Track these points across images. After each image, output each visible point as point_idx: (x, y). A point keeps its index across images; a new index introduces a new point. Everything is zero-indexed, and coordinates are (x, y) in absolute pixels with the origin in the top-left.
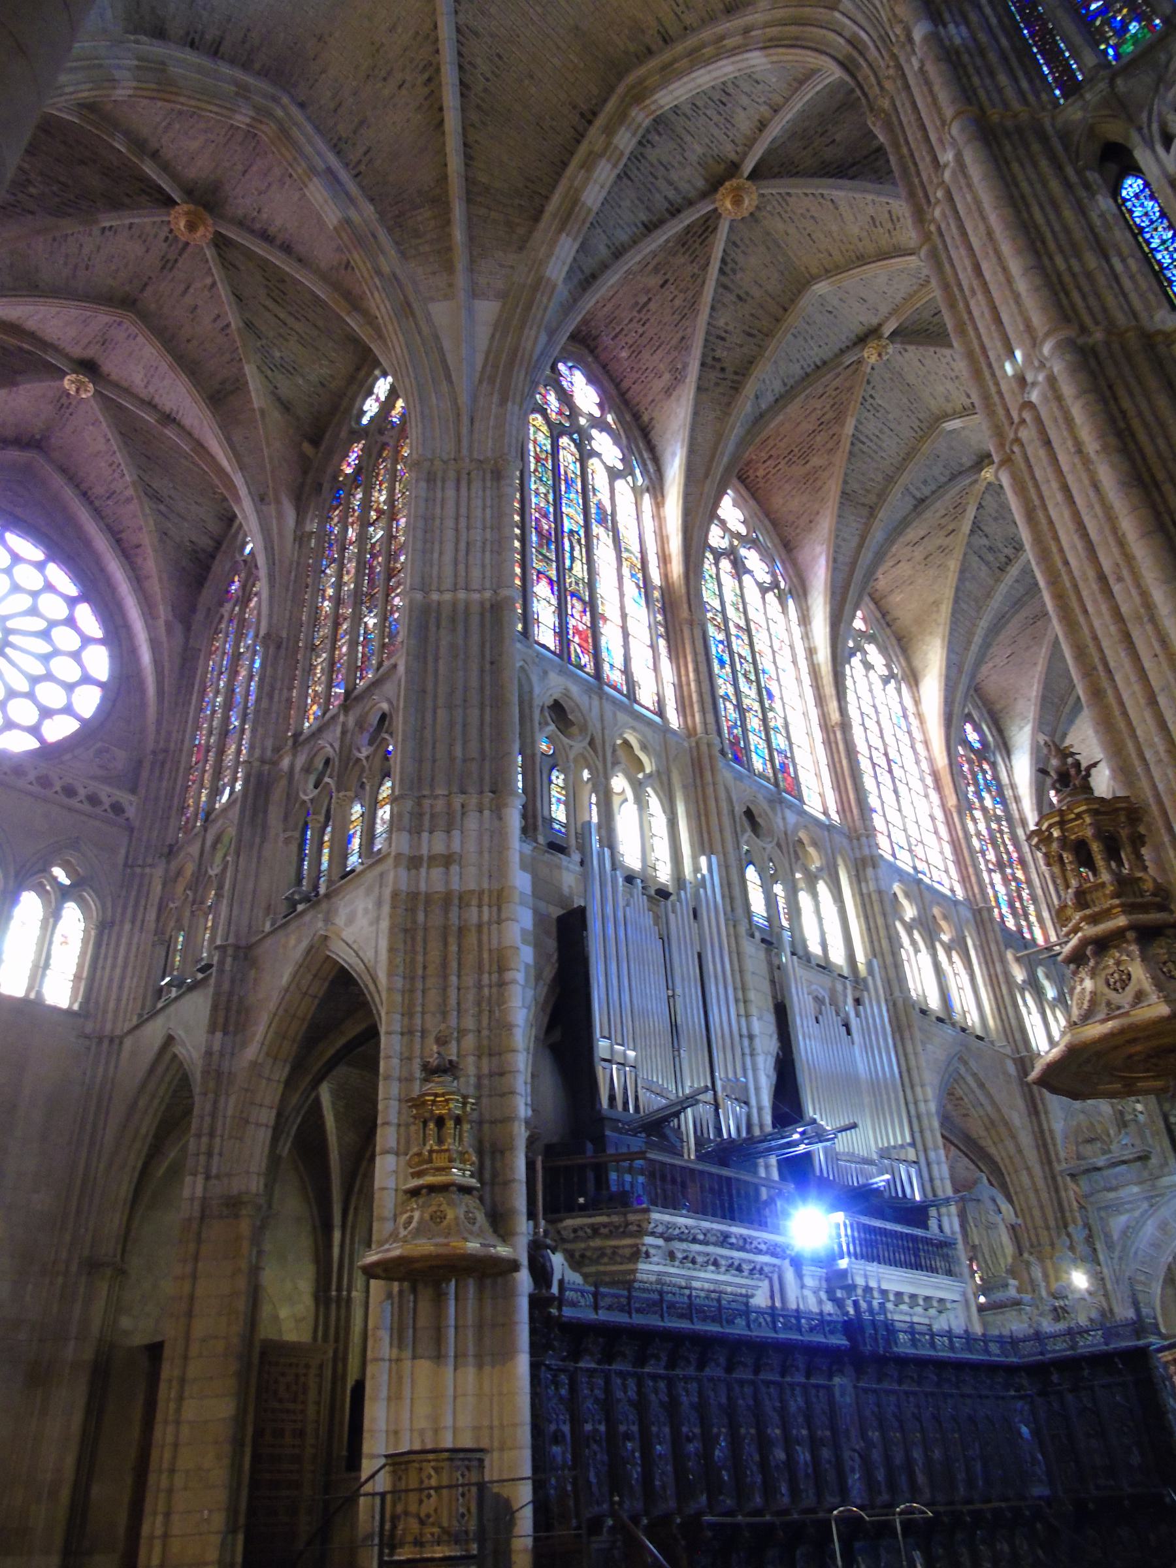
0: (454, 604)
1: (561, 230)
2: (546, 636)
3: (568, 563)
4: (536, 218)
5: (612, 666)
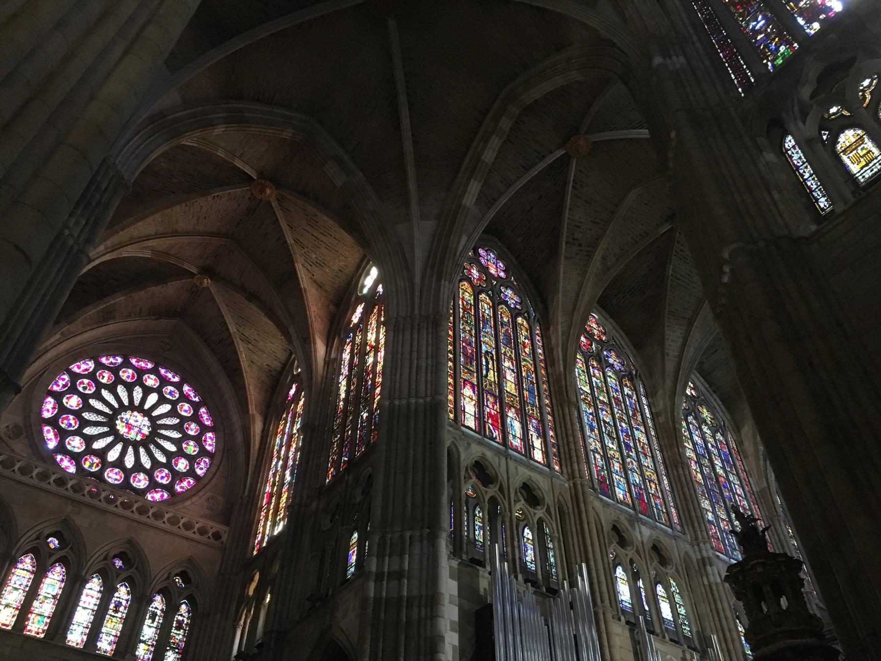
0: (409, 405)
1: (469, 179)
2: (471, 422)
3: (484, 372)
5: (514, 437)
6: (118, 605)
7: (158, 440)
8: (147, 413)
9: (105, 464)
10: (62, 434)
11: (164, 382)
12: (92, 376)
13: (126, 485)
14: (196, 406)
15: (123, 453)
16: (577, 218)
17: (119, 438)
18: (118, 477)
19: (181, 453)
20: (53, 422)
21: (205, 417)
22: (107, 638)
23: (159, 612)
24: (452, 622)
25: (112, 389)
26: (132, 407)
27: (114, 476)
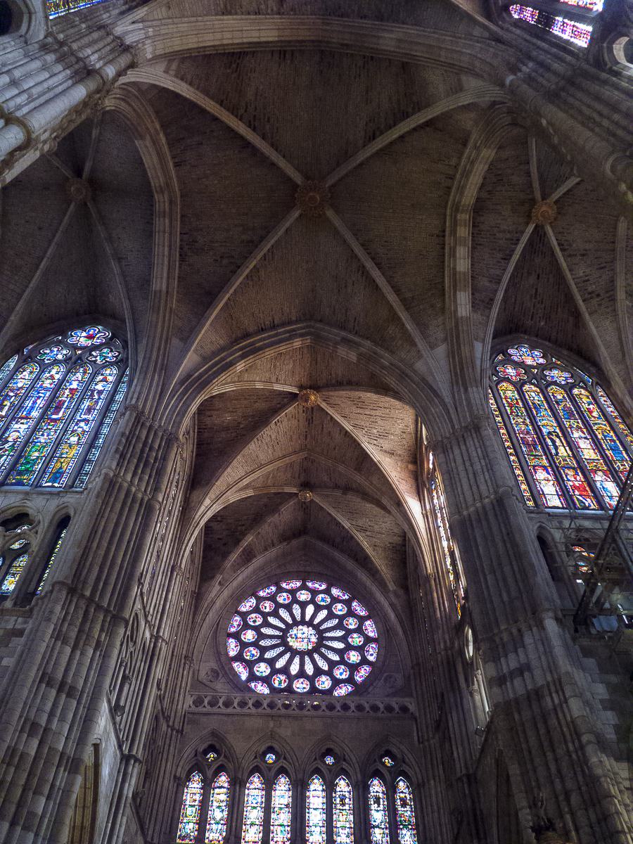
2: (554, 501)
3: (553, 451)
4: (443, 293)
6: (343, 799)
7: (327, 643)
8: (310, 624)
9: (291, 679)
10: (250, 665)
11: (314, 593)
12: (256, 610)
13: (313, 690)
14: (348, 603)
15: (302, 664)
16: (581, 274)
17: (295, 652)
18: (305, 686)
19: (349, 647)
20: (239, 658)
21: (358, 609)
22: (344, 831)
23: (381, 795)
24: (602, 701)
25: (275, 614)
26: (296, 623)
27: (301, 686)
